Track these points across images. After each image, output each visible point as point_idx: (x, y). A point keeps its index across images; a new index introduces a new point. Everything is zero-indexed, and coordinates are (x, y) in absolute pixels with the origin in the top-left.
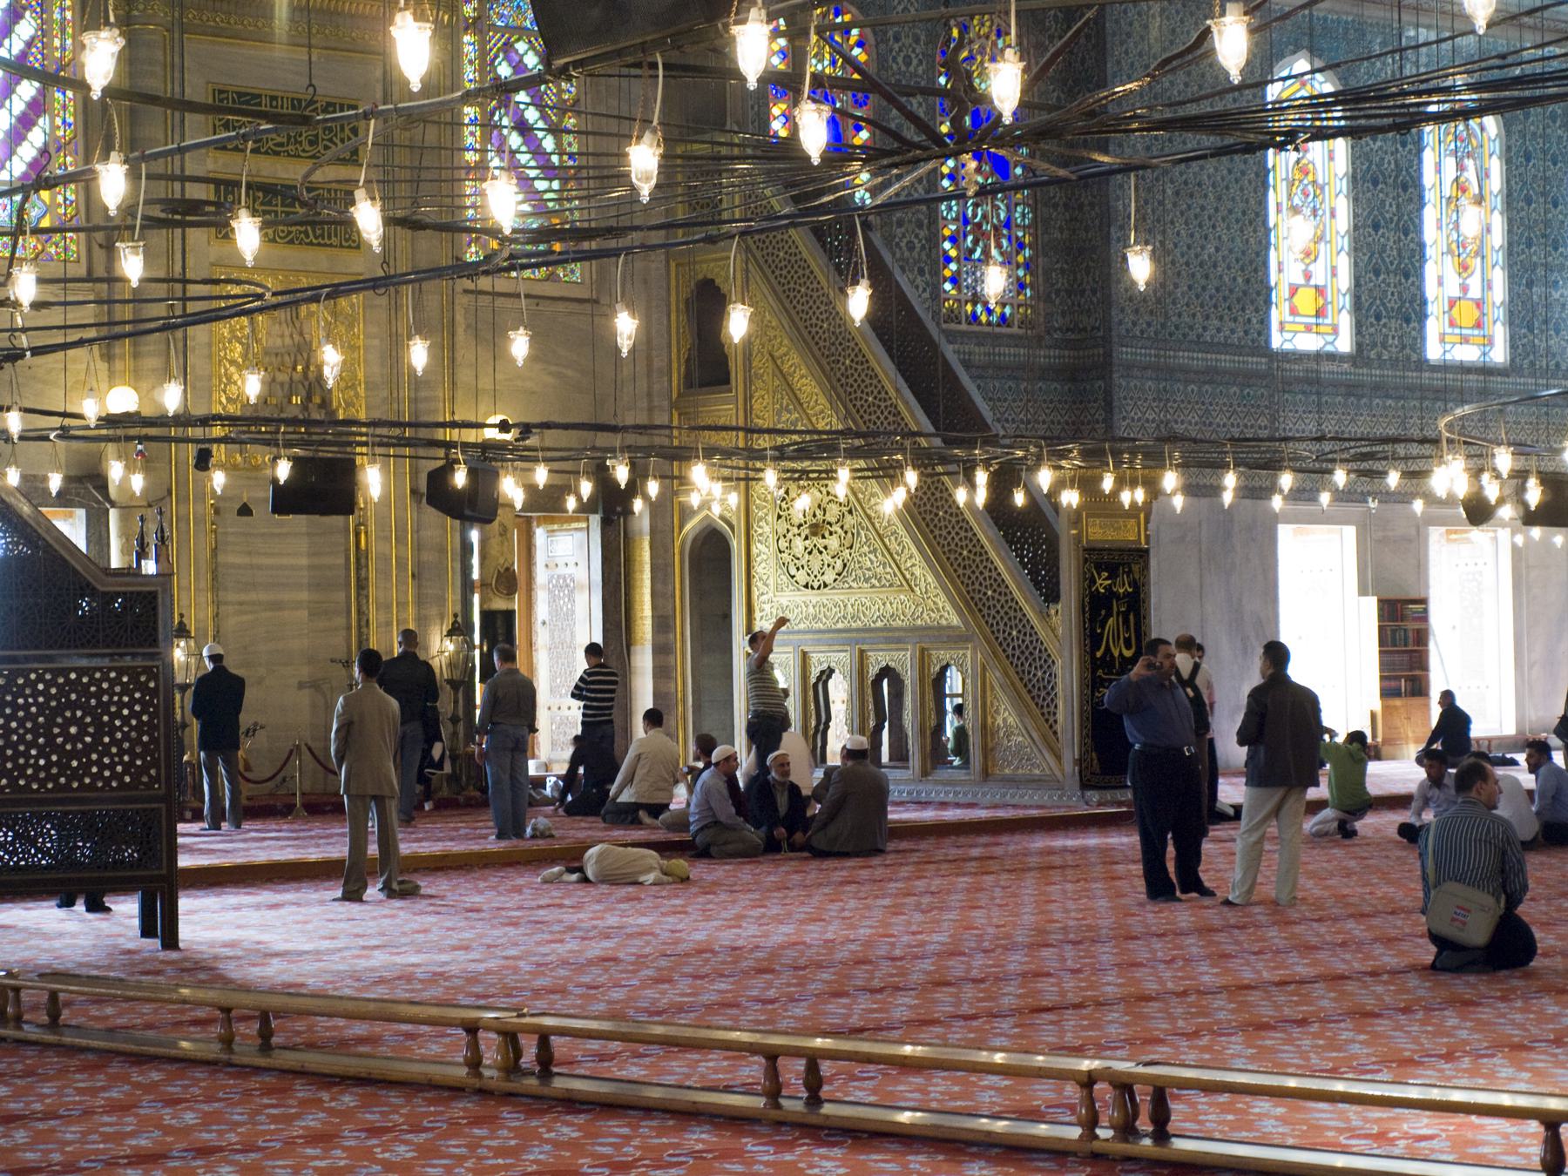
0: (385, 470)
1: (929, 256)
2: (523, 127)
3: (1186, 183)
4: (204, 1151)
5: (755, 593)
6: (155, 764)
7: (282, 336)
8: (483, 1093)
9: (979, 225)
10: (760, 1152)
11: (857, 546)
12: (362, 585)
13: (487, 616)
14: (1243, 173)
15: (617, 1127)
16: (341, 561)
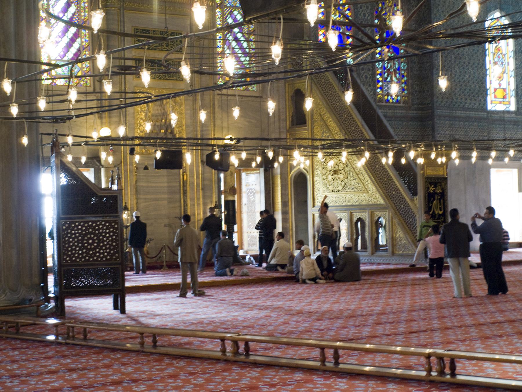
0: (192, 154)
1: (372, 80)
2: (236, 39)
3: (459, 54)
4: (135, 381)
5: (315, 193)
6: (117, 252)
7: (158, 110)
8: (227, 361)
9: (389, 70)
10: (319, 380)
11: (349, 178)
12: (185, 192)
13: (226, 202)
14: (478, 51)
15: (271, 372)
16: (178, 184)
